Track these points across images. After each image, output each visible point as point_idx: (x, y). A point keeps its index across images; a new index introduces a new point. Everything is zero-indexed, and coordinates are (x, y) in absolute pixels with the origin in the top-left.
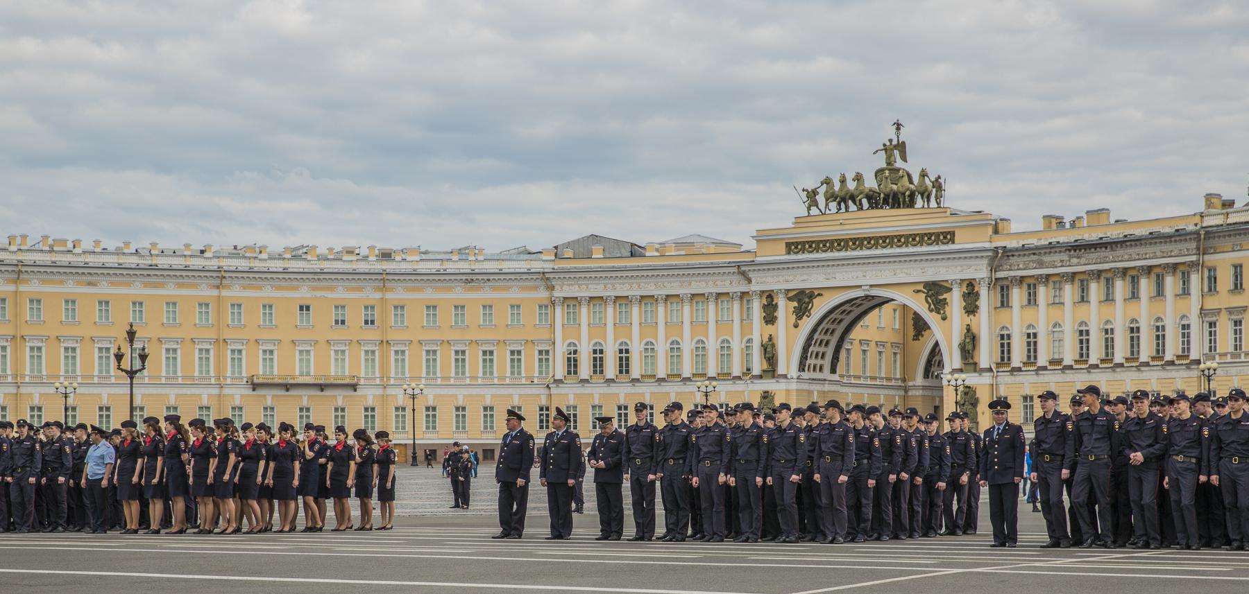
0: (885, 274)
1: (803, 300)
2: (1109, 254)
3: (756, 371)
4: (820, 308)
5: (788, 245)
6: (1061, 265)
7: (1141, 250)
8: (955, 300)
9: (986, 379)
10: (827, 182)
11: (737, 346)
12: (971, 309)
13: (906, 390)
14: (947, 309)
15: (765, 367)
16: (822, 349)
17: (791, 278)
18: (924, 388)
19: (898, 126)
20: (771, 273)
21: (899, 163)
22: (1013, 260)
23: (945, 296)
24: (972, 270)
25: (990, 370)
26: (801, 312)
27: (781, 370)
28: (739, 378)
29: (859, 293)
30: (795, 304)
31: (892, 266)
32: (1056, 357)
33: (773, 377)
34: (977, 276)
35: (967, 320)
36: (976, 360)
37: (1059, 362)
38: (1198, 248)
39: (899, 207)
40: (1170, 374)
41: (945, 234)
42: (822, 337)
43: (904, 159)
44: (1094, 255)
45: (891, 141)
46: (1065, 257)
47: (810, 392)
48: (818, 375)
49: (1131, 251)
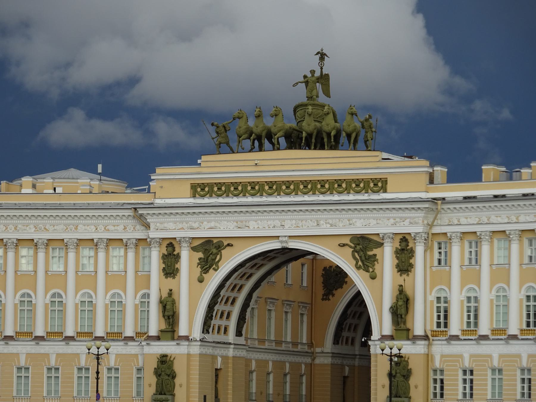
1: (210, 251)
3: (153, 332)
9: (420, 348)
11: (131, 300)
12: (404, 266)
13: (313, 355)
15: (163, 327)
16: (227, 308)
17: (196, 225)
18: (334, 355)
19: (322, 56)
20: (172, 218)
21: (322, 99)
23: (375, 251)
24: (407, 222)
25: (426, 337)
26: (208, 264)
27: (183, 330)
28: (131, 339)
29: (275, 245)
30: (201, 255)
33: (173, 339)
34: (412, 230)
35: (400, 280)
36: (409, 326)
37: (503, 331)
39: (322, 148)
41: (375, 182)
42: (229, 294)
43: (327, 94)
45: (313, 72)
47: (214, 357)
48: (221, 338)
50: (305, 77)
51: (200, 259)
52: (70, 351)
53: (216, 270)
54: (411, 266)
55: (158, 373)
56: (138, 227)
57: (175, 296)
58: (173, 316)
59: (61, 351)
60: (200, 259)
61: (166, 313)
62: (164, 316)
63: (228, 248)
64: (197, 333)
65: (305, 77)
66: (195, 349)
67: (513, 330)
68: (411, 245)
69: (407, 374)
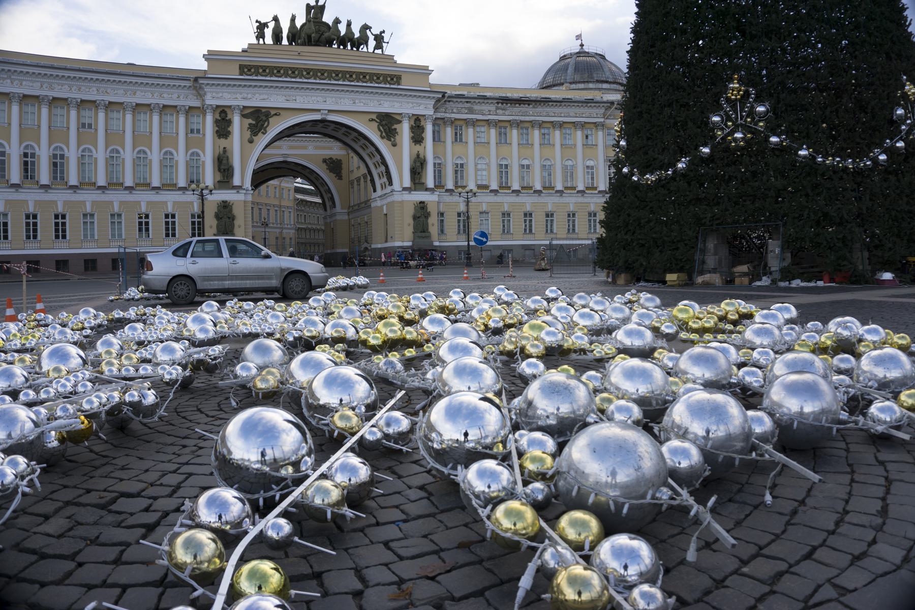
0: (346, 103)
1: (258, 119)
2: (530, 110)
4: (276, 127)
5: (242, 68)
6: (489, 112)
7: (557, 110)
8: (405, 130)
10: (276, 19)
12: (417, 137)
14: (397, 137)
15: (219, 178)
17: (249, 96)
20: (230, 89)
22: (448, 105)
23: (395, 126)
24: (422, 107)
27: (236, 181)
29: (317, 117)
31: (352, 95)
32: (479, 183)
33: (229, 188)
37: (486, 187)
38: (604, 115)
40: (586, 200)
41: (392, 77)
44: (517, 109)
46: (492, 108)
49: (548, 109)
50: (308, 5)
51: (250, 124)
52: (132, 199)
53: (264, 134)
54: (423, 139)
55: (218, 216)
56: (191, 96)
57: (228, 154)
58: (228, 170)
59: (124, 199)
60: (250, 124)
61: (222, 167)
62: (219, 170)
63: (275, 117)
64: (248, 184)
65: (308, 5)
66: (250, 198)
67: (494, 186)
68: (422, 123)
69: (427, 215)
